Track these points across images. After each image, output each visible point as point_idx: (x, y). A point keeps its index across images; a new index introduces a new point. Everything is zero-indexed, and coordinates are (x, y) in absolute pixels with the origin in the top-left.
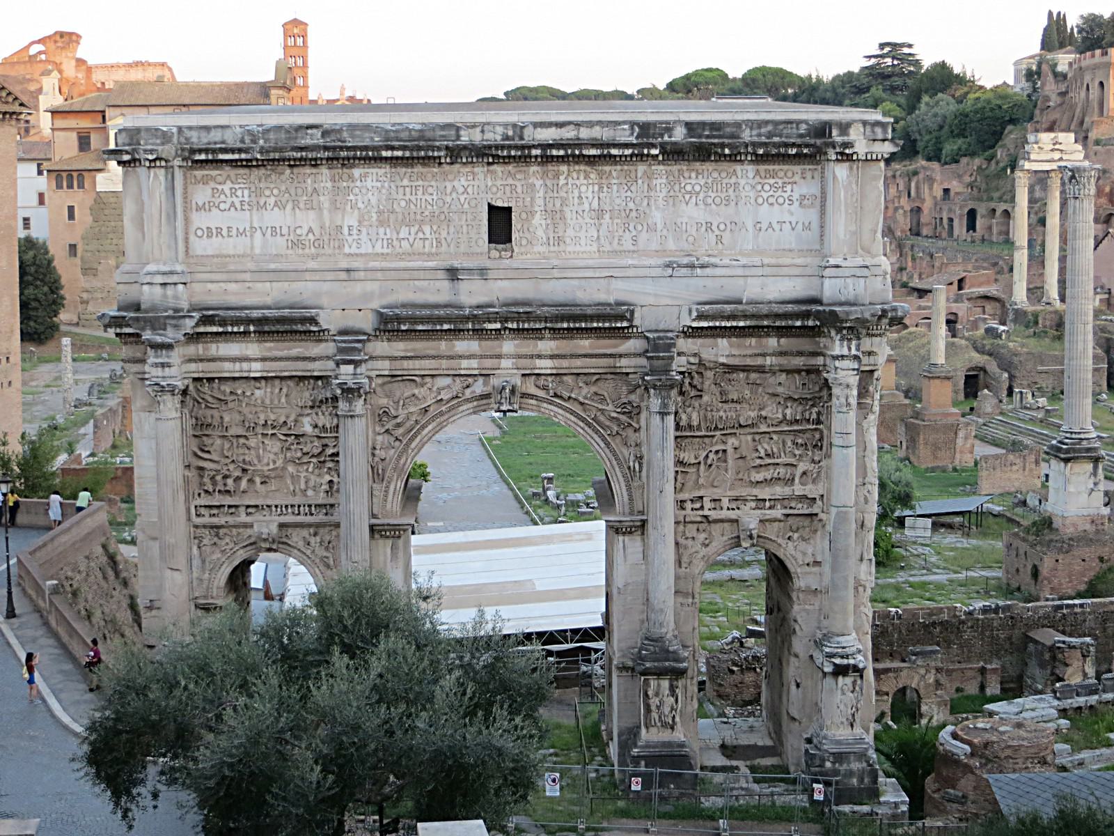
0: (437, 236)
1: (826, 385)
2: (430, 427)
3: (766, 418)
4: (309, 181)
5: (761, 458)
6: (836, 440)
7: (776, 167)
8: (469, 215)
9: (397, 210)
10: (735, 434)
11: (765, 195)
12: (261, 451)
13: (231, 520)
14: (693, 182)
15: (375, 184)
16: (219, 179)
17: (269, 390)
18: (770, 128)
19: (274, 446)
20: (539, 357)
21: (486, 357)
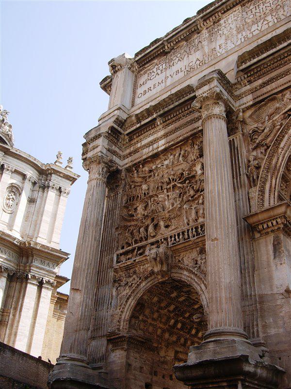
13: (138, 259)
19: (173, 194)
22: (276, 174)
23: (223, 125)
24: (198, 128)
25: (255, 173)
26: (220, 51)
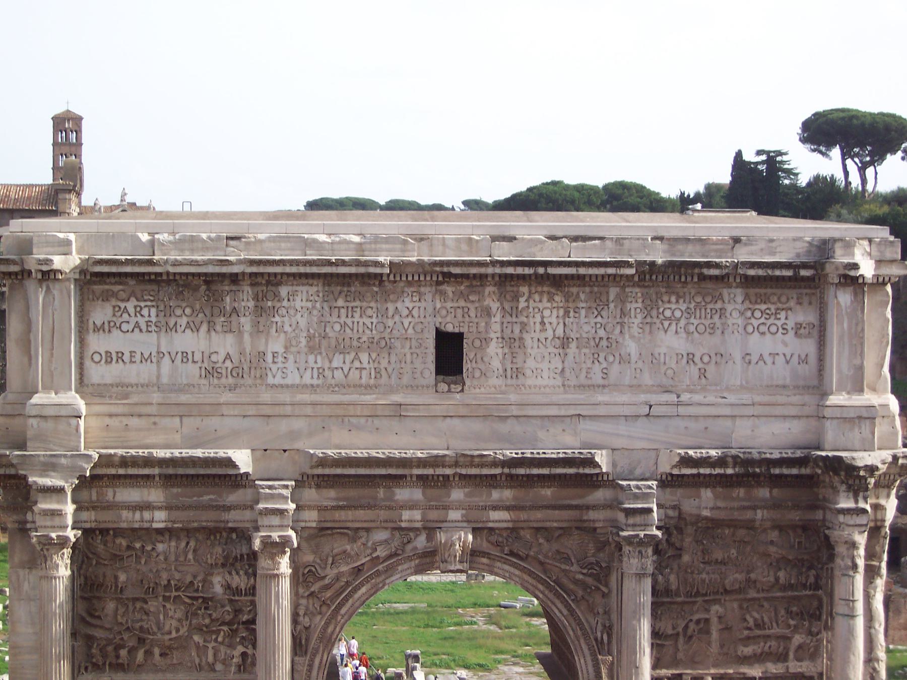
0: (376, 365)
1: (828, 546)
2: (364, 590)
3: (755, 582)
4: (228, 299)
5: (749, 629)
6: (840, 608)
7: (769, 291)
8: (413, 341)
9: (330, 335)
10: (720, 599)
11: (755, 323)
12: (162, 617)
14: (673, 306)
15: (304, 304)
16: (123, 295)
17: (173, 544)
18: (762, 245)
19: (176, 612)
20: (495, 508)
21: (431, 508)
24: (228, 522)
25: (304, 637)
26: (274, 368)
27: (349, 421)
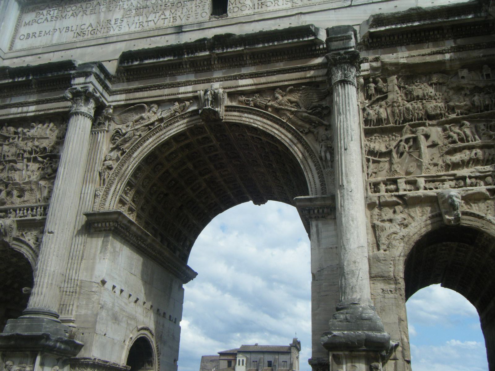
0: (174, 15)
2: (150, 140)
5: (454, 142)
19: (34, 166)
20: (242, 77)
22: (123, 180)
23: (88, 123)
26: (115, 26)
27: (150, 40)
